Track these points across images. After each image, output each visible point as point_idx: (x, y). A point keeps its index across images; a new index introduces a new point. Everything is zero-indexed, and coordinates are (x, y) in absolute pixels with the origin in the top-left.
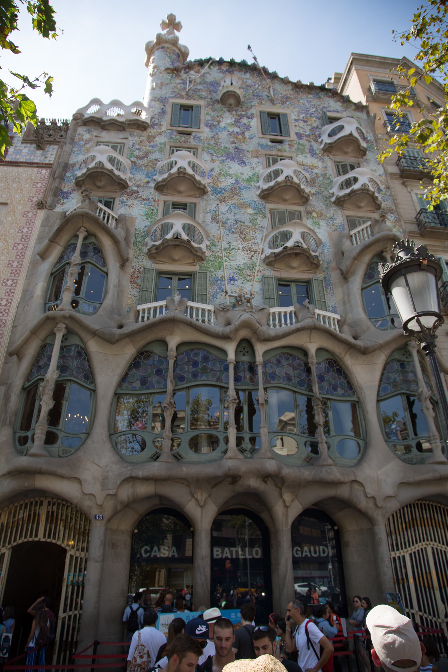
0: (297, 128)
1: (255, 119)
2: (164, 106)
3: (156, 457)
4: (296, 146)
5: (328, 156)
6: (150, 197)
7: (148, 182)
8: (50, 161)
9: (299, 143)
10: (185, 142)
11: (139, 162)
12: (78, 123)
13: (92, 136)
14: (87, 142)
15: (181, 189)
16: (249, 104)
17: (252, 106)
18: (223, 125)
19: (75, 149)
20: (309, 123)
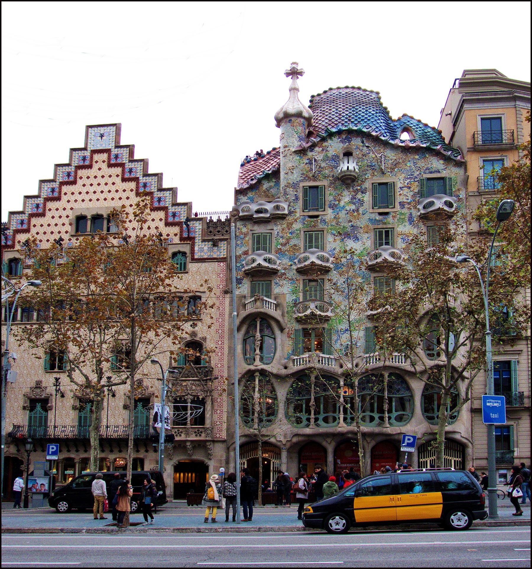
0: (402, 197)
1: (368, 193)
2: (297, 191)
3: (308, 426)
4: (398, 216)
5: (423, 222)
6: (294, 277)
7: (291, 265)
8: (224, 255)
9: (401, 213)
10: (314, 227)
11: (284, 248)
12: (236, 219)
13: (248, 229)
14: (246, 235)
15: (313, 275)
16: (363, 177)
17: (366, 179)
18: (342, 204)
19: (239, 242)
20: (412, 189)
